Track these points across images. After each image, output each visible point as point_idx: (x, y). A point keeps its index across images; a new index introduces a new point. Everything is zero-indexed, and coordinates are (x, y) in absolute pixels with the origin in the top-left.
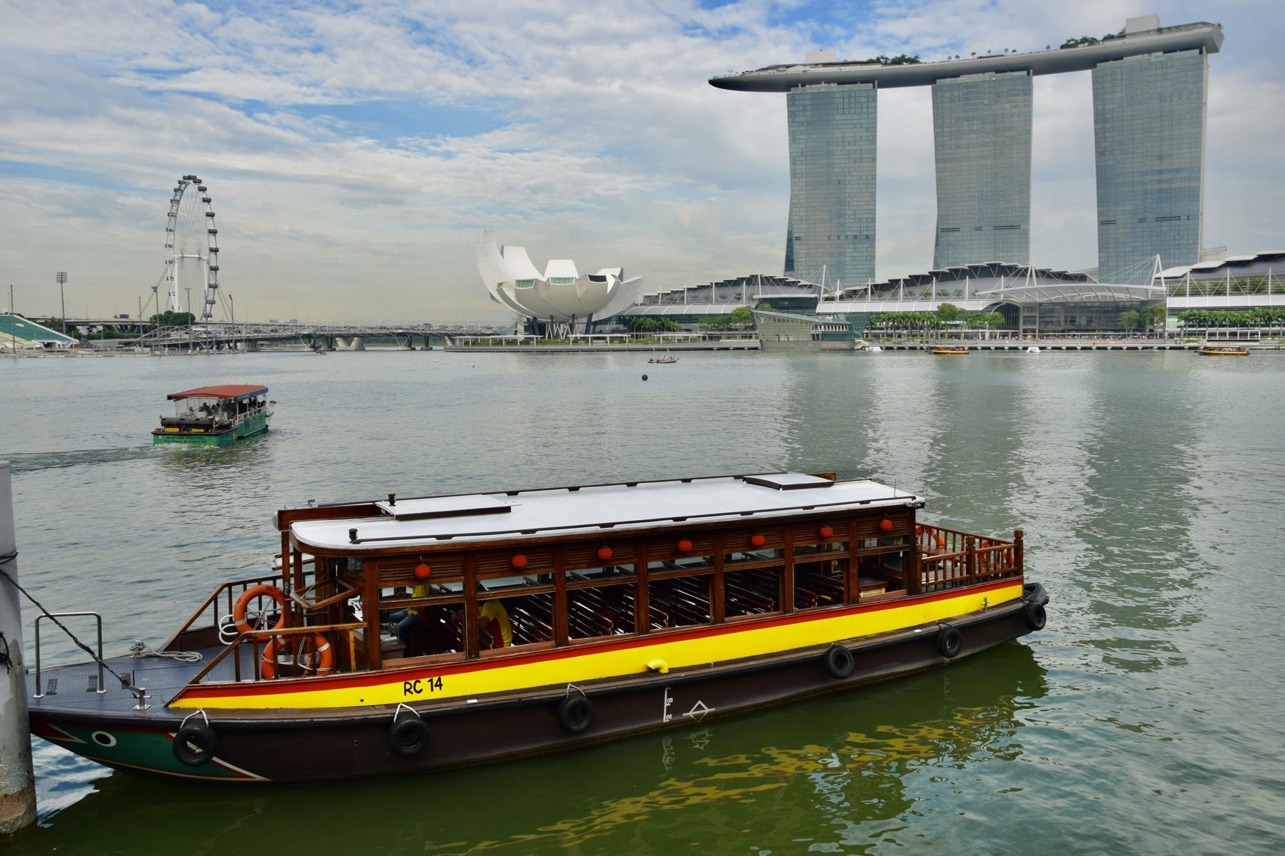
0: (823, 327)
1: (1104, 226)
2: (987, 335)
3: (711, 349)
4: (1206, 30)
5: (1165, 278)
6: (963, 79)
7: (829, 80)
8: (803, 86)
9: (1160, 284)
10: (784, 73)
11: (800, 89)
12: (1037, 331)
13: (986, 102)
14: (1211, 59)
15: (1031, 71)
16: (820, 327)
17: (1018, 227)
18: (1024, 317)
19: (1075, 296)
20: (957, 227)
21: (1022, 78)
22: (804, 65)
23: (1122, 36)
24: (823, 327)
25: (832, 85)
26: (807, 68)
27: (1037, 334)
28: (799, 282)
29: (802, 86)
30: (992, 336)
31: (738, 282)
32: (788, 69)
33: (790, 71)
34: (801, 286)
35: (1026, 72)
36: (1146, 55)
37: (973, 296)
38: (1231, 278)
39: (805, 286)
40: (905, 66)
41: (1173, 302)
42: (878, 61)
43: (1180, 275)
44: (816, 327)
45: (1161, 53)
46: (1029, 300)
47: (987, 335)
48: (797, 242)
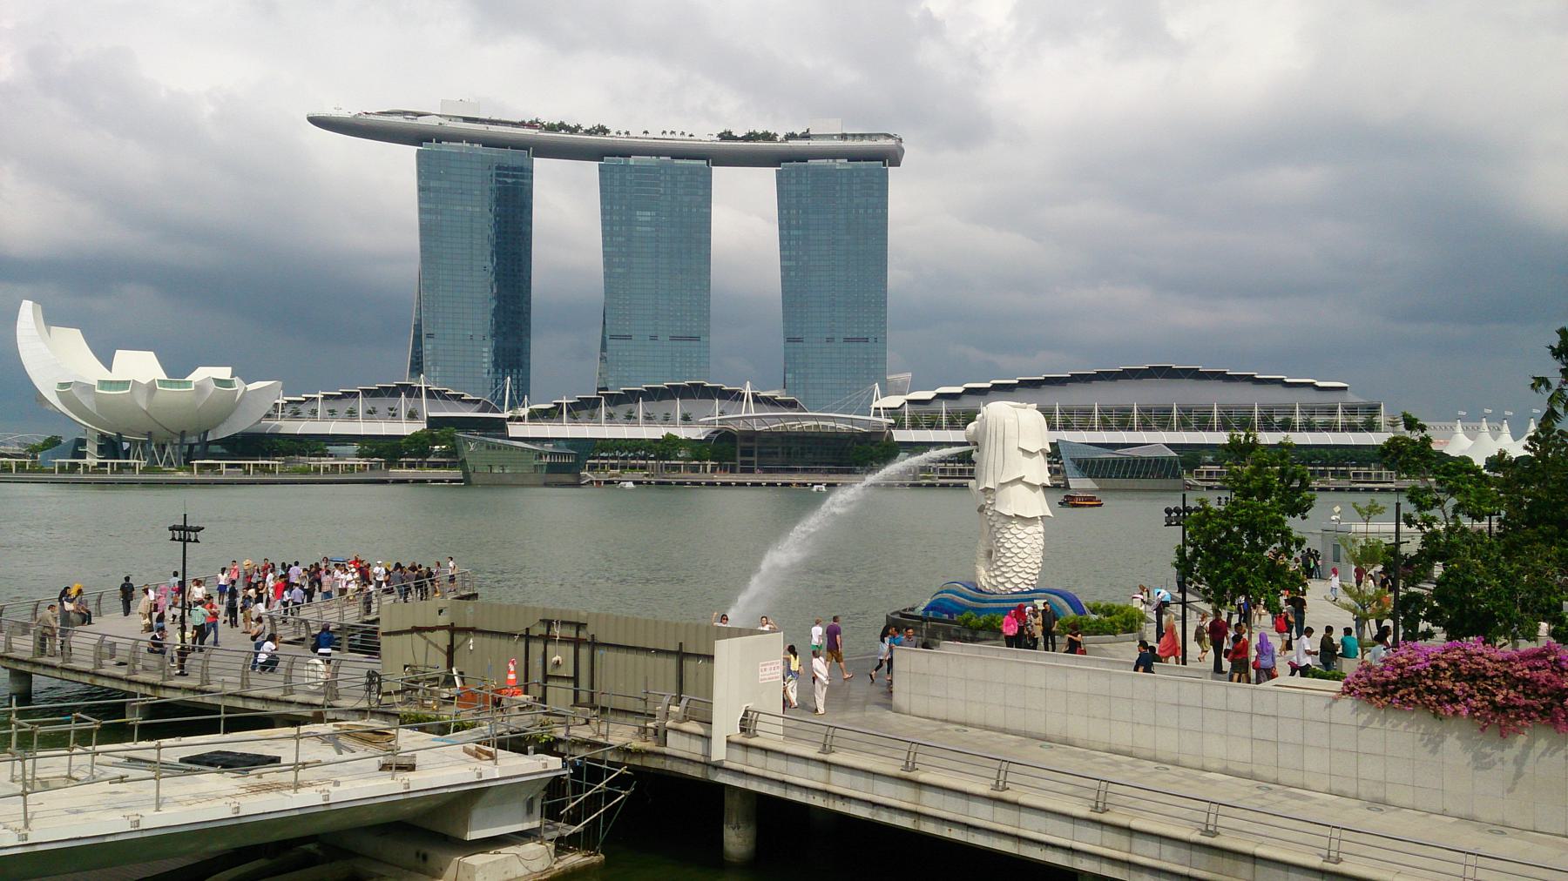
0: (548, 457)
1: (792, 343)
2: (709, 470)
3: (405, 481)
4: (891, 142)
5: (884, 409)
6: (632, 160)
7: (472, 139)
8: (439, 141)
9: (880, 415)
10: (415, 122)
11: (433, 146)
12: (756, 464)
13: (662, 190)
14: (892, 171)
15: (710, 161)
16: (546, 457)
17: (697, 339)
18: (741, 447)
19: (793, 425)
20: (627, 334)
21: (701, 167)
22: (440, 116)
23: (806, 136)
24: (548, 457)
25: (476, 145)
26: (444, 121)
27: (756, 467)
28: (463, 395)
29: (436, 142)
30: (713, 470)
31: (394, 392)
32: (419, 118)
33: (421, 121)
34: (465, 401)
35: (705, 162)
36: (831, 161)
37: (686, 418)
38: (947, 412)
39: (471, 401)
40: (563, 135)
41: (899, 436)
42: (531, 125)
43: (898, 406)
44: (541, 457)
45: (846, 161)
46: (749, 428)
47: (709, 470)
48: (431, 340)
